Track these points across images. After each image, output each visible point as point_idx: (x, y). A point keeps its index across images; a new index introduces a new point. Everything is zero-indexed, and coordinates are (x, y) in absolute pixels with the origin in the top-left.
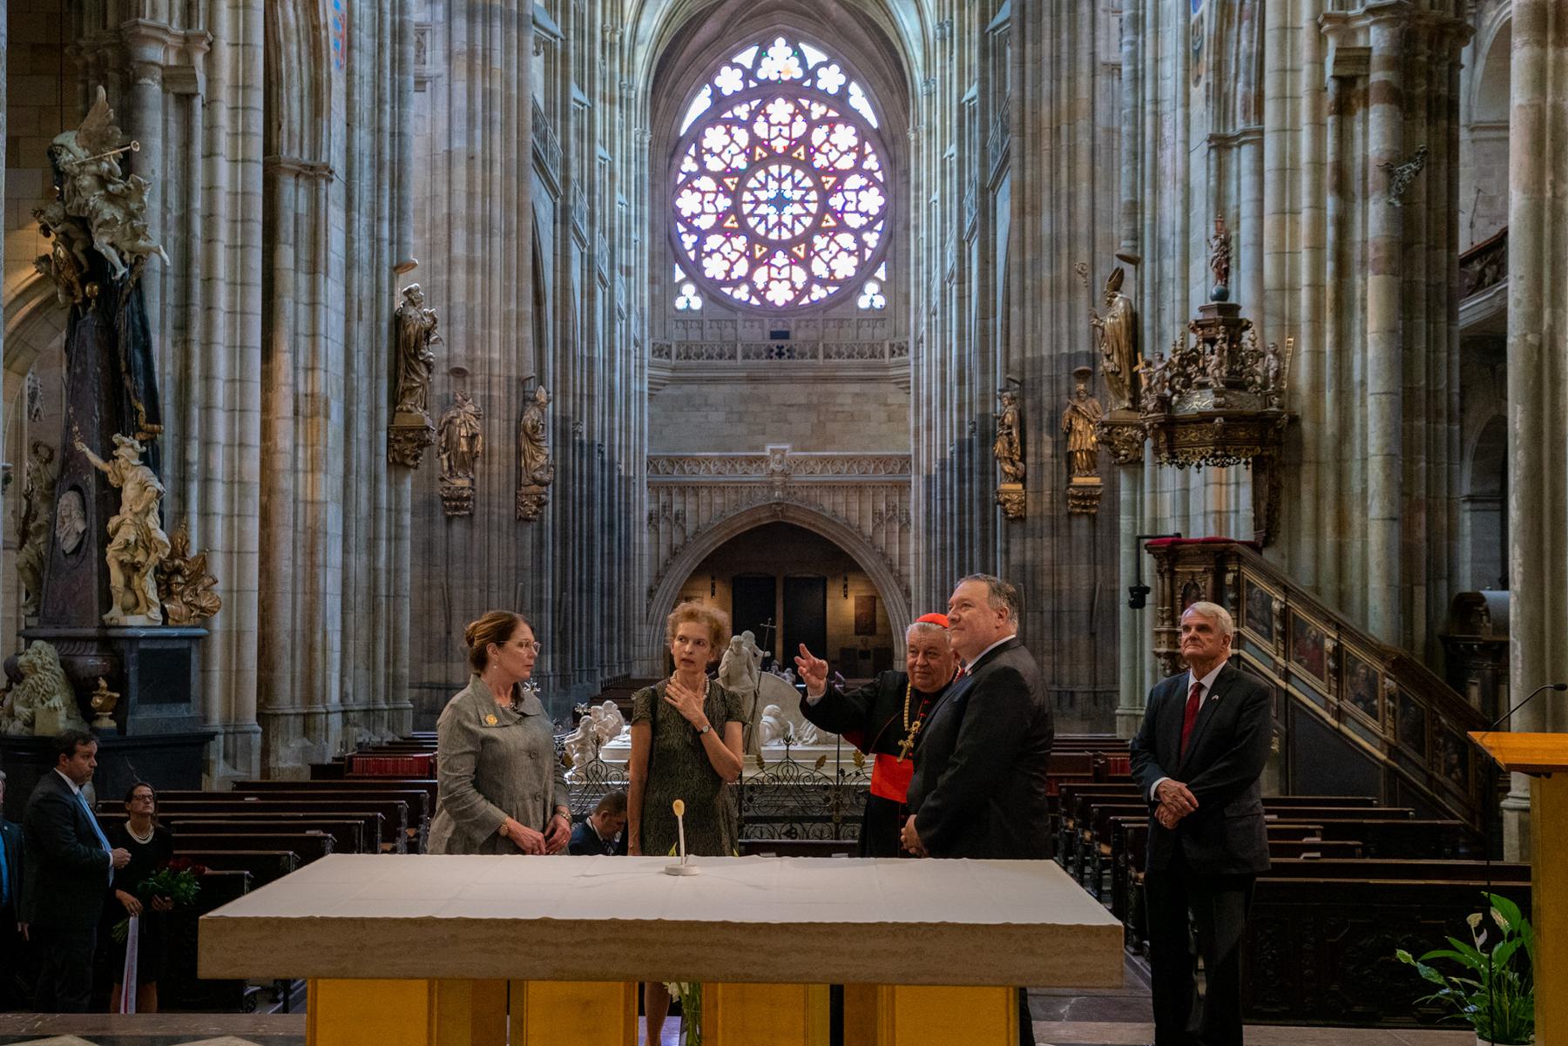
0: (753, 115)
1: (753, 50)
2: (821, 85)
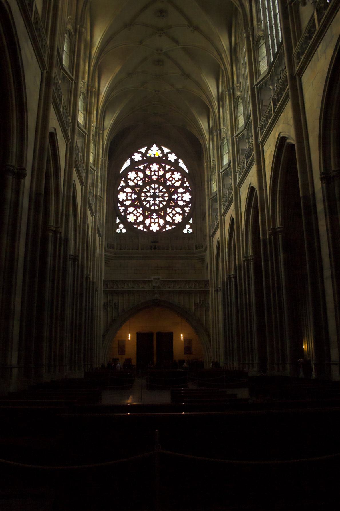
0: (145, 168)
1: (145, 148)
2: (169, 159)
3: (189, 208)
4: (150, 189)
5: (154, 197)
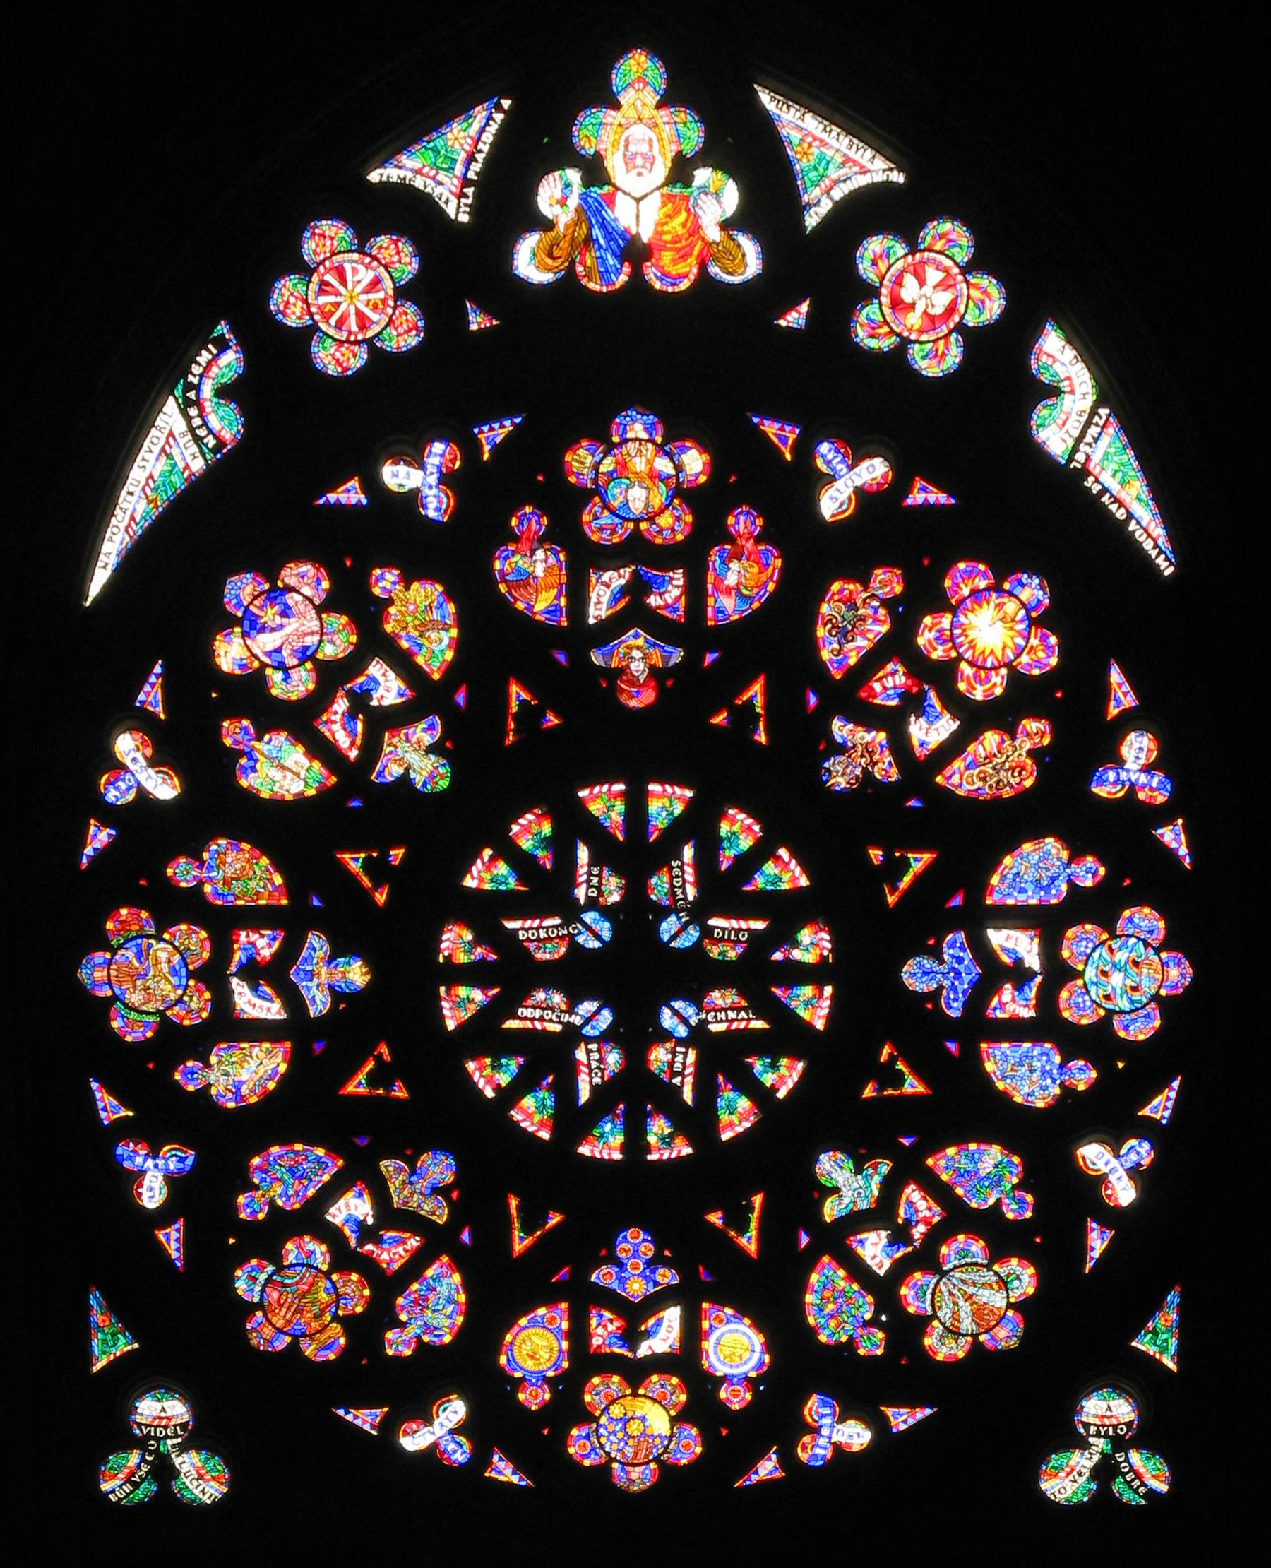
2: (870, 329)
3: (1140, 1151)
4: (561, 846)
5: (635, 975)
